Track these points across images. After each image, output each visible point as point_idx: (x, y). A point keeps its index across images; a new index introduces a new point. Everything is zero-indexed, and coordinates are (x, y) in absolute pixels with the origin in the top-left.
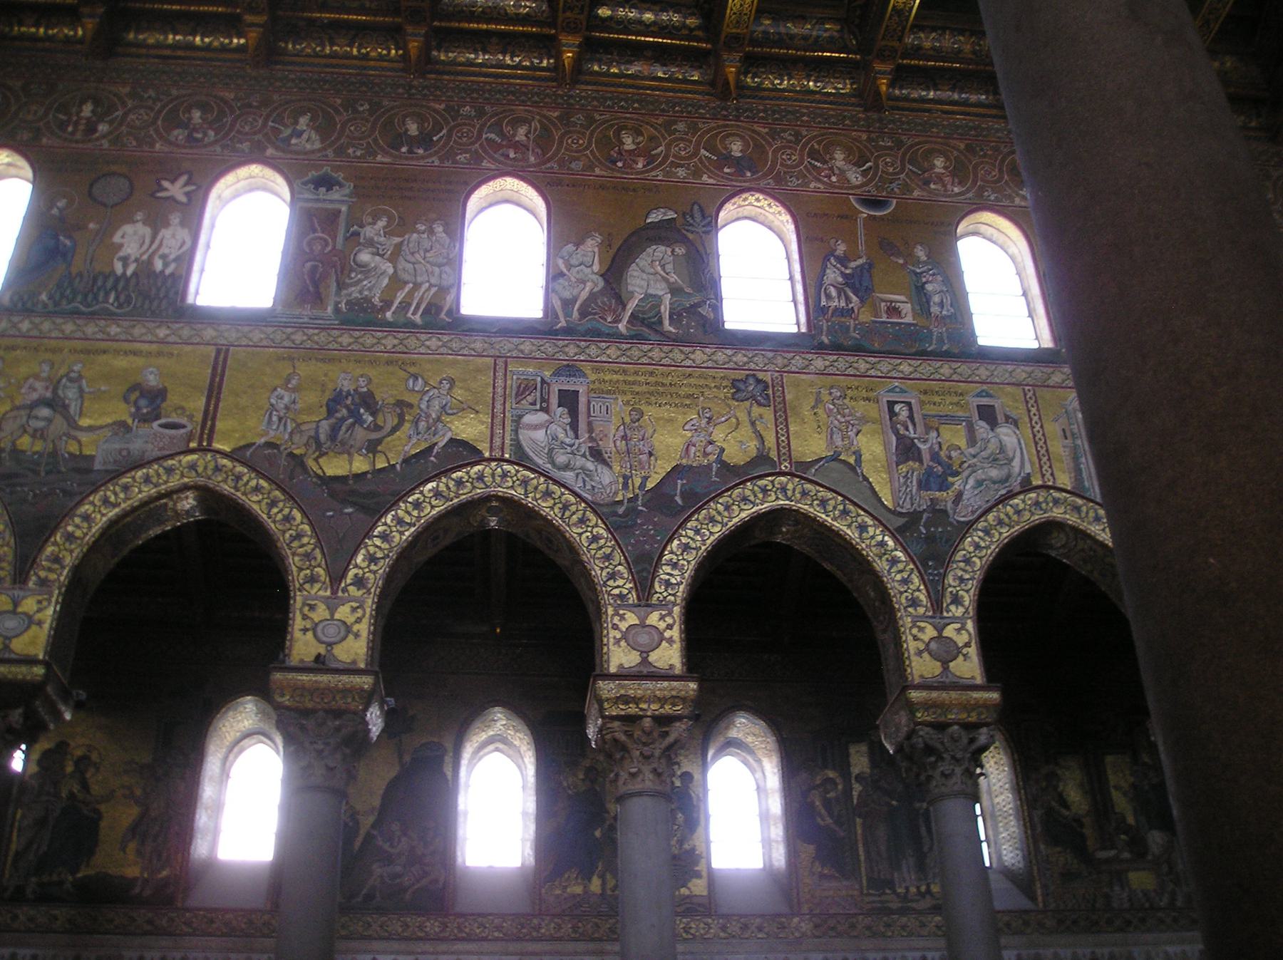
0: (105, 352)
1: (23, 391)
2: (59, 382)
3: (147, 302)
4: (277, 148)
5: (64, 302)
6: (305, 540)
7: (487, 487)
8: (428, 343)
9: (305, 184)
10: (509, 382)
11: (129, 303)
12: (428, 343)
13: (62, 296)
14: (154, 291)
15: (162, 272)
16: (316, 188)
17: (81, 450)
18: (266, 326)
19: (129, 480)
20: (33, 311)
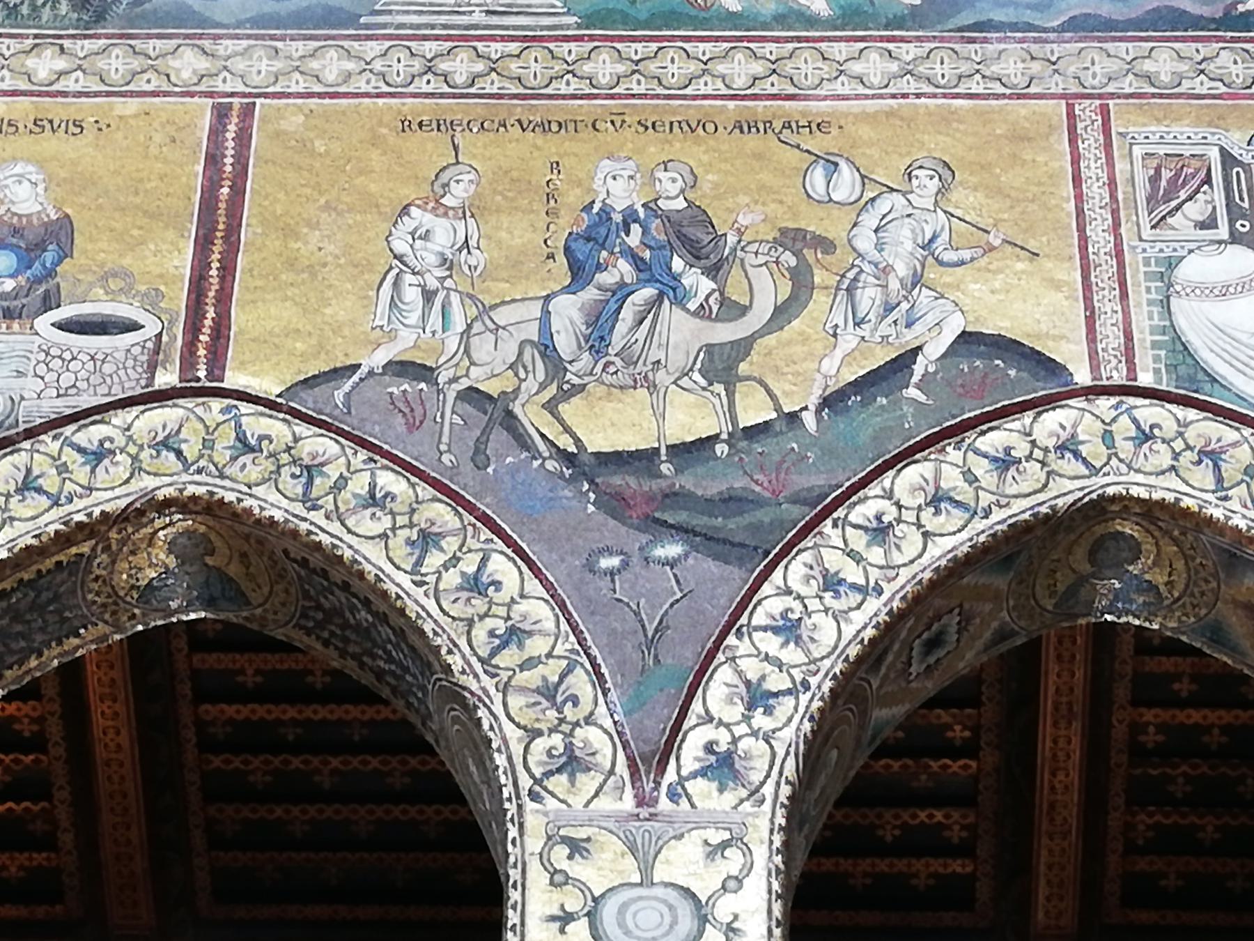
6: (536, 646)
7: (1095, 471)
8: (856, 68)
10: (1121, 166)
12: (856, 68)
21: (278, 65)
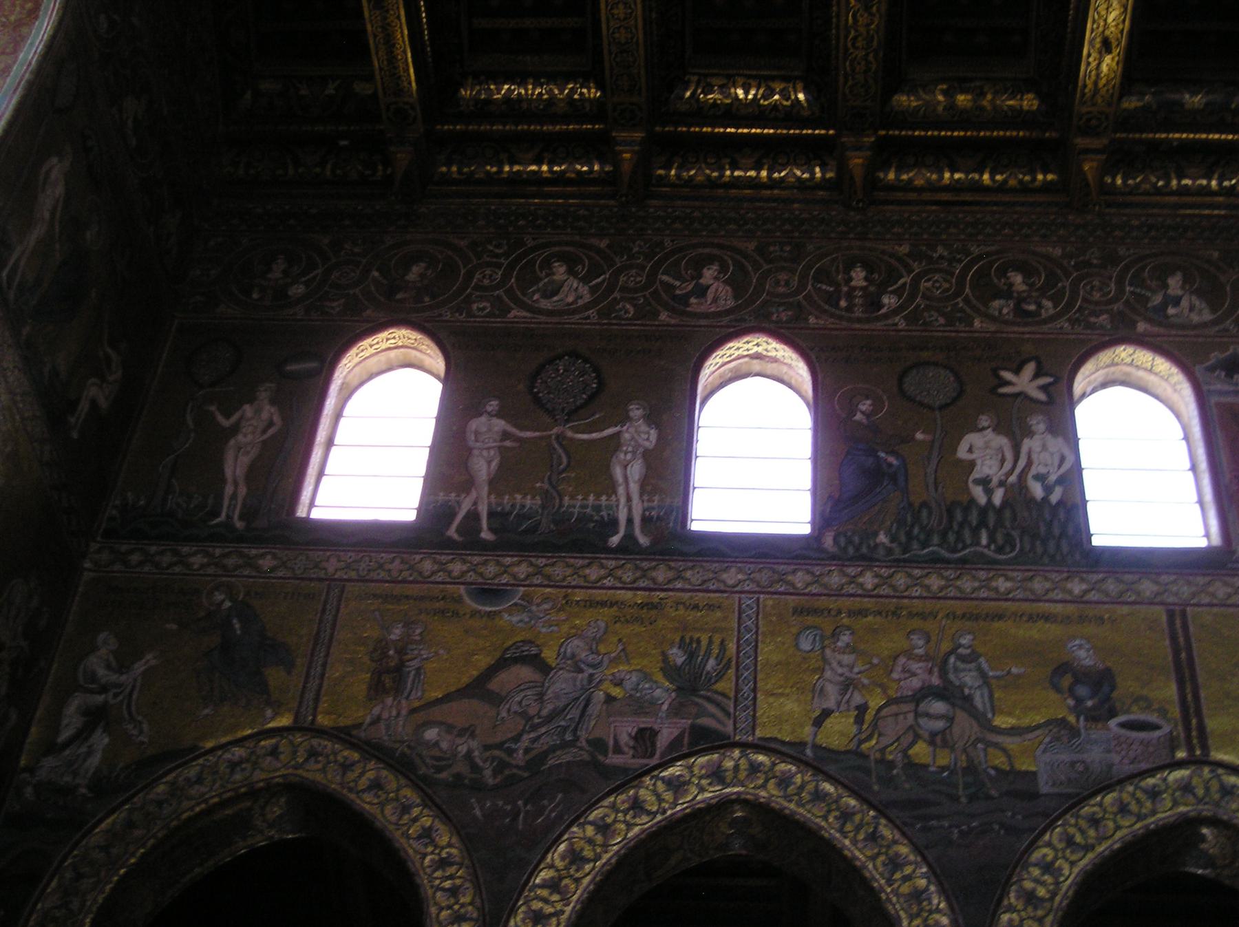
0: (1000, 617)
1: (895, 675)
2: (945, 661)
3: (1038, 543)
5: (915, 545)
9: (1212, 369)
11: (1013, 548)
13: (909, 535)
14: (1043, 529)
15: (1045, 500)
17: (1011, 765)
19: (1096, 809)
20: (871, 559)
21: (1194, 589)
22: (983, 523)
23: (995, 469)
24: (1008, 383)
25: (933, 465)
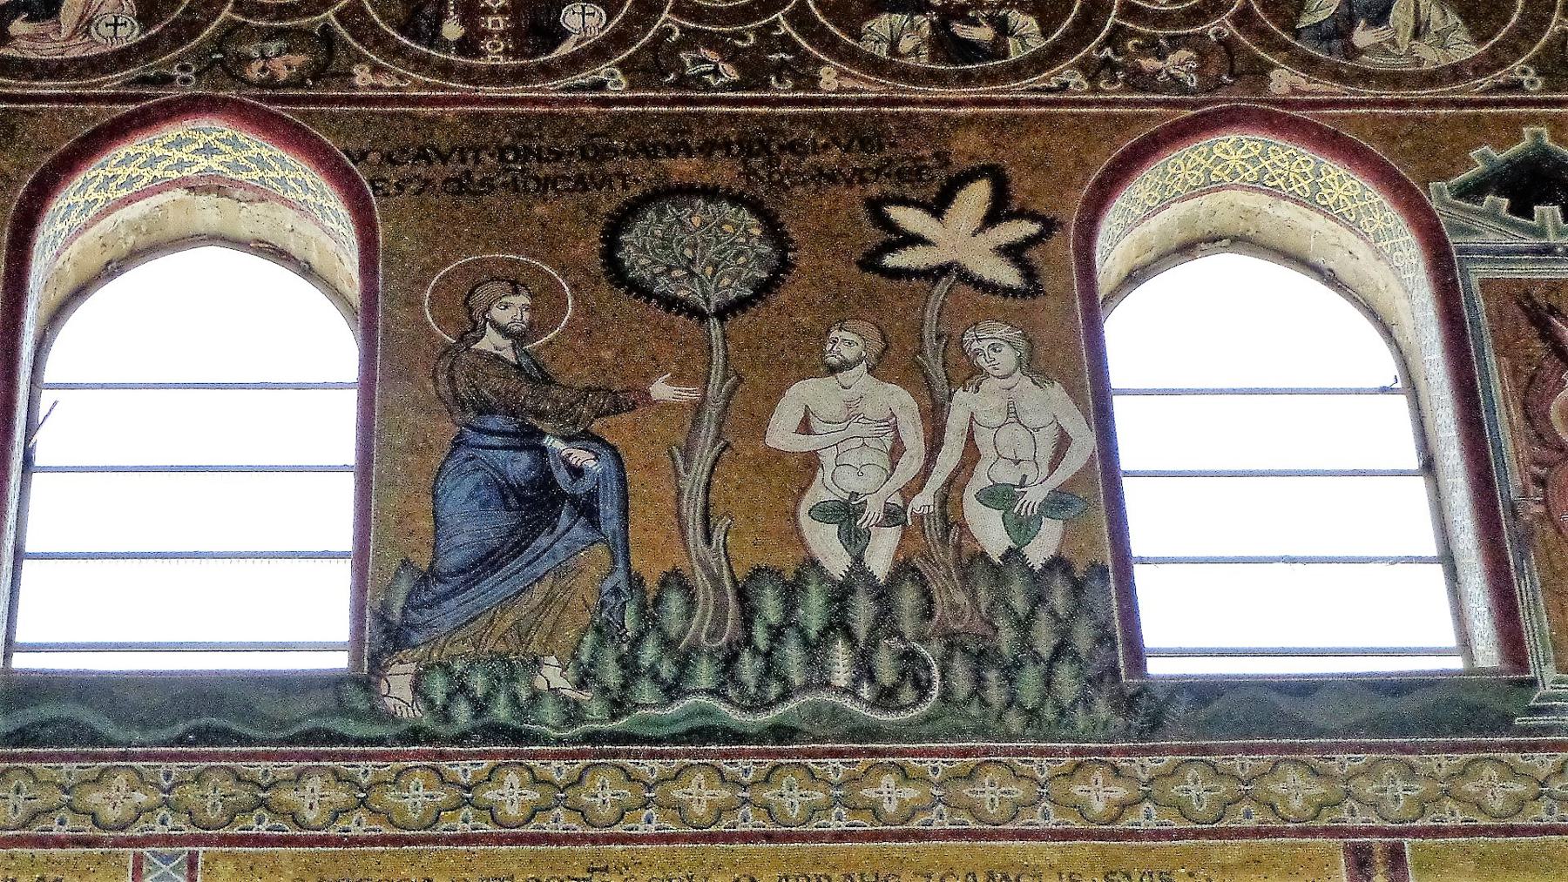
3: (992, 675)
4: (1308, 64)
5: (646, 692)
9: (1473, 191)
11: (922, 689)
13: (630, 667)
14: (1006, 638)
15: (1012, 555)
16: (1522, 208)
18: (1518, 748)
20: (519, 737)
21: (1420, 788)
22: (839, 625)
23: (873, 476)
24: (914, 240)
25: (700, 469)
